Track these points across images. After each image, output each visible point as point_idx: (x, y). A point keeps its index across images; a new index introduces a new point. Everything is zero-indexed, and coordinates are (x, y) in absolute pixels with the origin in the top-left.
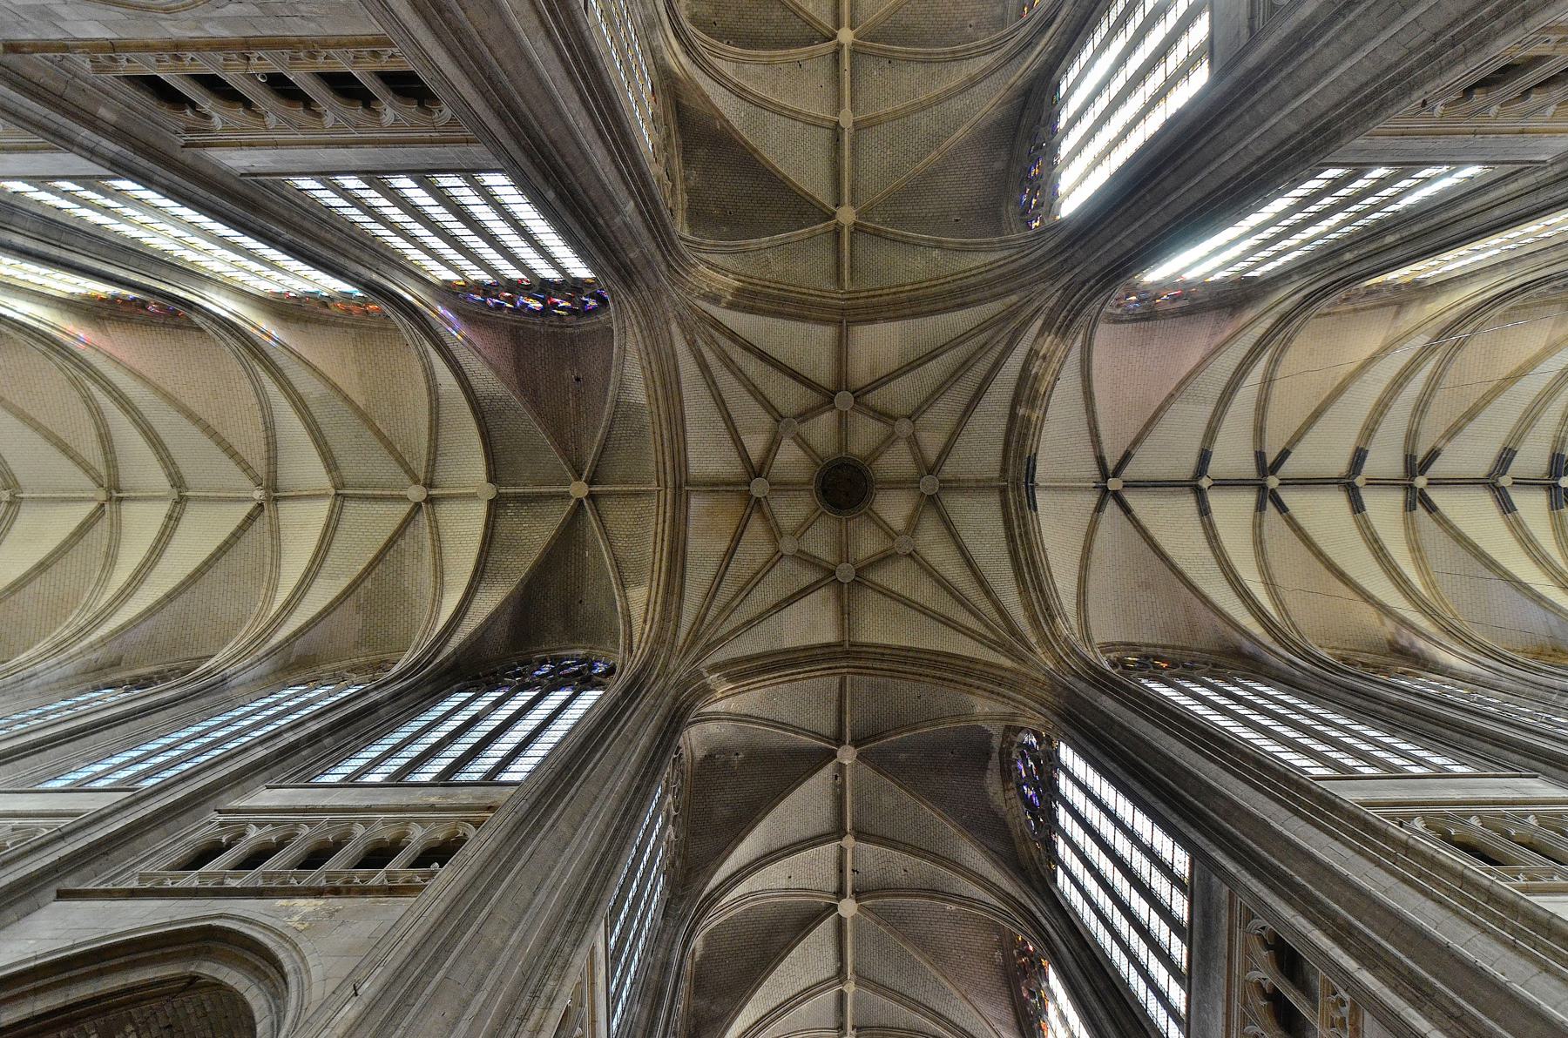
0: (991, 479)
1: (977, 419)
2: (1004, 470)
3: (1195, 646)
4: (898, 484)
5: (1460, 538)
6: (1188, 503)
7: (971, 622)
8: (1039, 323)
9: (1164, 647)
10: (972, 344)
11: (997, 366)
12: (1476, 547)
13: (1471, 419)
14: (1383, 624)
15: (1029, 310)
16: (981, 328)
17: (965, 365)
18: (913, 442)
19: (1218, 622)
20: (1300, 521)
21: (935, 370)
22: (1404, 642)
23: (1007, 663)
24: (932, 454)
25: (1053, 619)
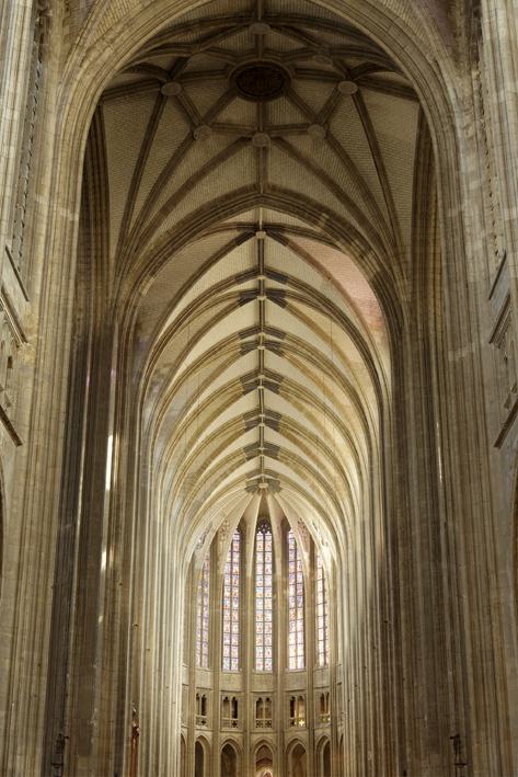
0: (266, 177)
1: (319, 183)
2: (274, 188)
4: (263, 114)
5: (223, 367)
7: (139, 204)
8: (386, 267)
10: (382, 205)
11: (362, 220)
14: (165, 366)
15: (396, 268)
16: (395, 221)
17: (368, 195)
18: (301, 129)
19: (157, 315)
21: (367, 164)
23: (113, 254)
24: (293, 139)
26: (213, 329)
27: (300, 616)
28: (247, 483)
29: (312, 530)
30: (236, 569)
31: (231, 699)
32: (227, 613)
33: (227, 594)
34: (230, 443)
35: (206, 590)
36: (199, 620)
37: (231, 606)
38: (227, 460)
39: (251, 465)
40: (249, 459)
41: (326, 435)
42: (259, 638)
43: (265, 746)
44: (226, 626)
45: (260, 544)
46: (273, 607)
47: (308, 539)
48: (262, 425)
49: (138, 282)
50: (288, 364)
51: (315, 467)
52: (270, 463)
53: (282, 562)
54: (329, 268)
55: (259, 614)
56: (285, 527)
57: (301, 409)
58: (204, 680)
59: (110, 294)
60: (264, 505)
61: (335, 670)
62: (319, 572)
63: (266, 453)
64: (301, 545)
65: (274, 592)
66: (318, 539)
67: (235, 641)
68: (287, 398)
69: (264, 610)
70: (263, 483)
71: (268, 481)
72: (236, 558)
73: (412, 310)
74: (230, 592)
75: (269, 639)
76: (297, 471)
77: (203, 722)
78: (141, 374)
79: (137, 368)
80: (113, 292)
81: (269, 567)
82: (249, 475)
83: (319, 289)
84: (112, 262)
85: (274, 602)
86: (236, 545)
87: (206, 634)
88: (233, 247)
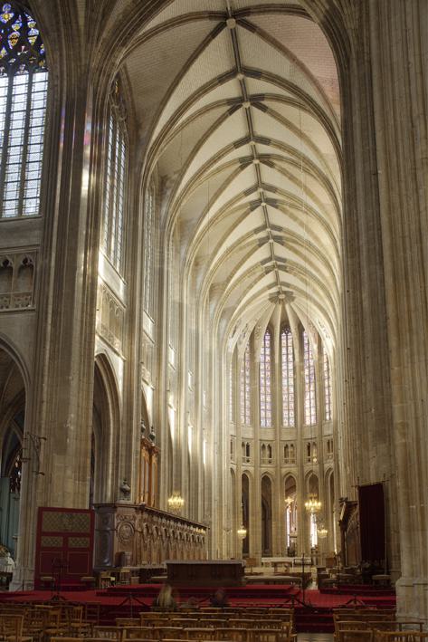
3: (134, 96)
5: (228, 181)
6: (225, 67)
9: (128, 78)
12: (224, 188)
13: (290, 178)
14: (175, 173)
20: (224, 124)
22: (168, 184)
23: (82, 21)
25: (124, 45)
26: (211, 139)
27: (312, 388)
28: (270, 294)
29: (318, 327)
30: (268, 358)
31: (267, 445)
32: (263, 389)
33: (262, 376)
34: (248, 257)
35: (247, 373)
36: (242, 394)
37: (265, 383)
38: (249, 271)
39: (270, 278)
40: (267, 273)
41: (316, 238)
42: (285, 405)
43: (291, 477)
44: (262, 397)
45: (284, 342)
46: (295, 383)
47: (316, 335)
48: (271, 241)
49: (110, 51)
50: (279, 174)
51: (314, 272)
52: (284, 276)
53: (299, 352)
54: (292, 51)
55: (285, 388)
56: (301, 329)
57: (295, 219)
58: (248, 434)
59: (83, 60)
60: (284, 309)
61: (336, 423)
62: (325, 357)
63: (279, 267)
64: (312, 340)
65: (294, 373)
66: (323, 334)
67: (268, 407)
68: (284, 211)
69: (288, 386)
70: (282, 296)
71: (285, 293)
72: (268, 352)
73: (359, 37)
74: (264, 373)
75: (292, 405)
76: (302, 280)
77: (248, 461)
78: (142, 164)
79: (139, 160)
80: (86, 58)
81: (290, 357)
82: (270, 287)
83: (287, 78)
84: (82, 28)
85: (294, 380)
86: (268, 342)
87: (248, 403)
88: (210, 40)
